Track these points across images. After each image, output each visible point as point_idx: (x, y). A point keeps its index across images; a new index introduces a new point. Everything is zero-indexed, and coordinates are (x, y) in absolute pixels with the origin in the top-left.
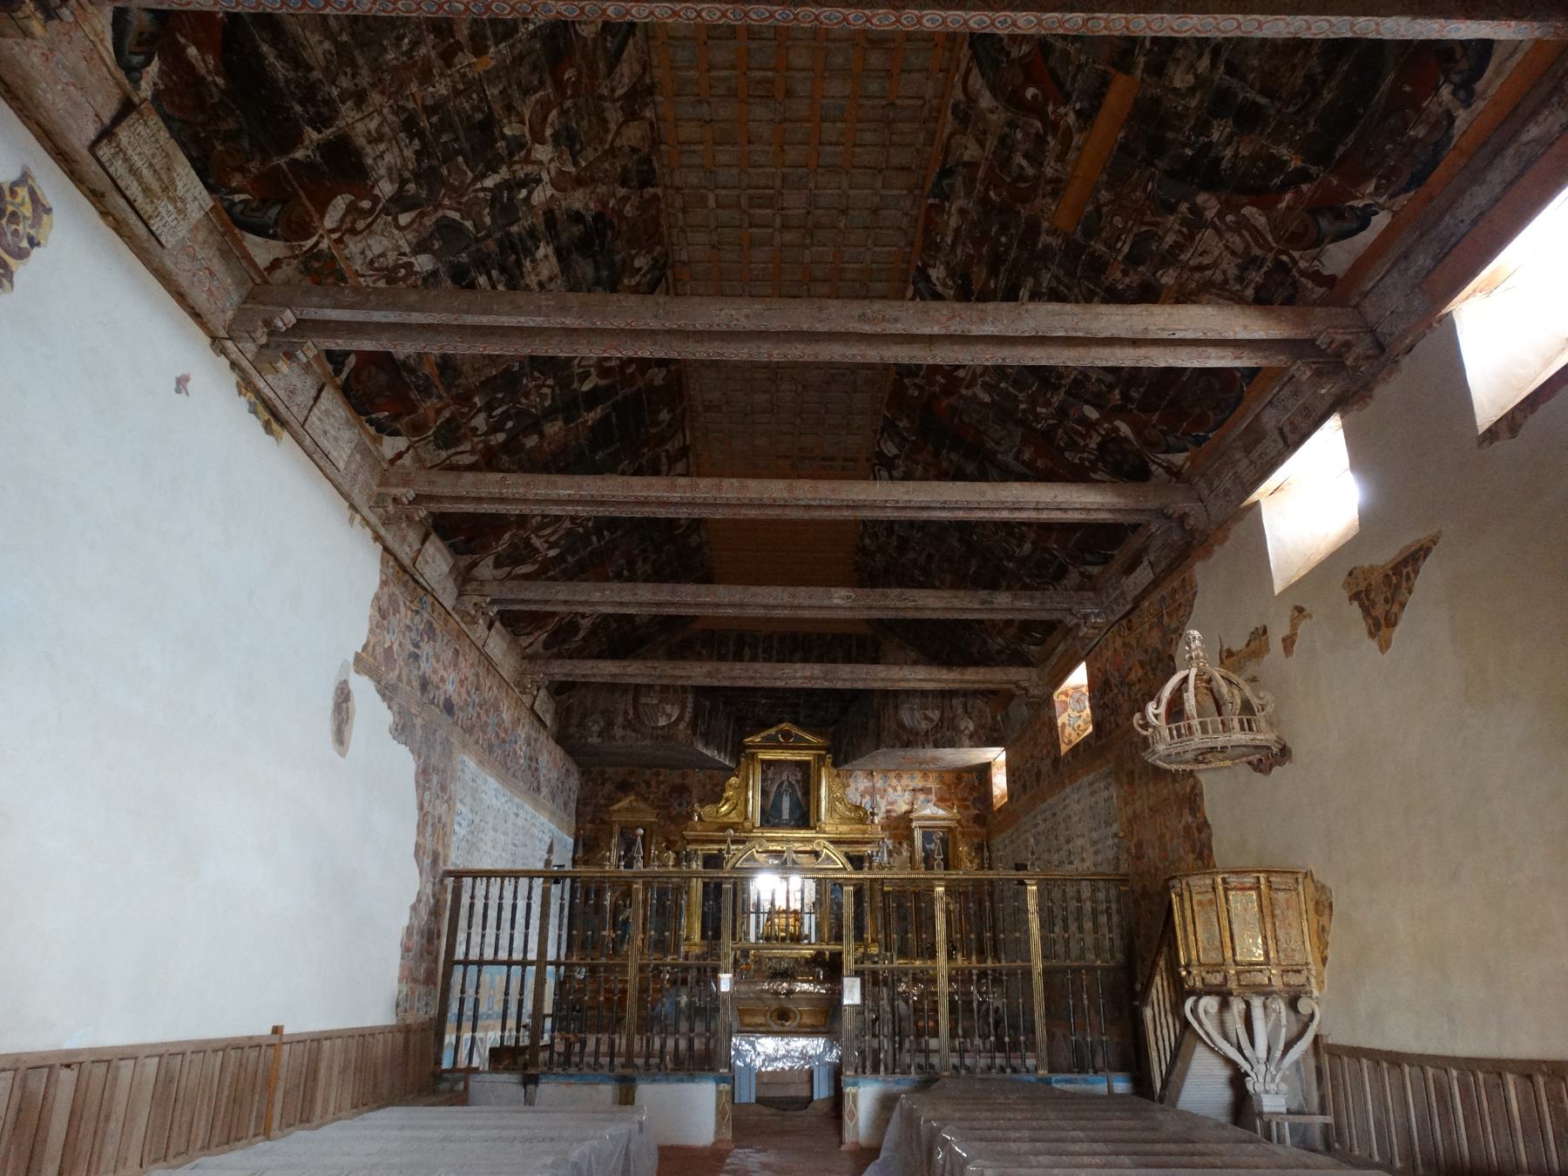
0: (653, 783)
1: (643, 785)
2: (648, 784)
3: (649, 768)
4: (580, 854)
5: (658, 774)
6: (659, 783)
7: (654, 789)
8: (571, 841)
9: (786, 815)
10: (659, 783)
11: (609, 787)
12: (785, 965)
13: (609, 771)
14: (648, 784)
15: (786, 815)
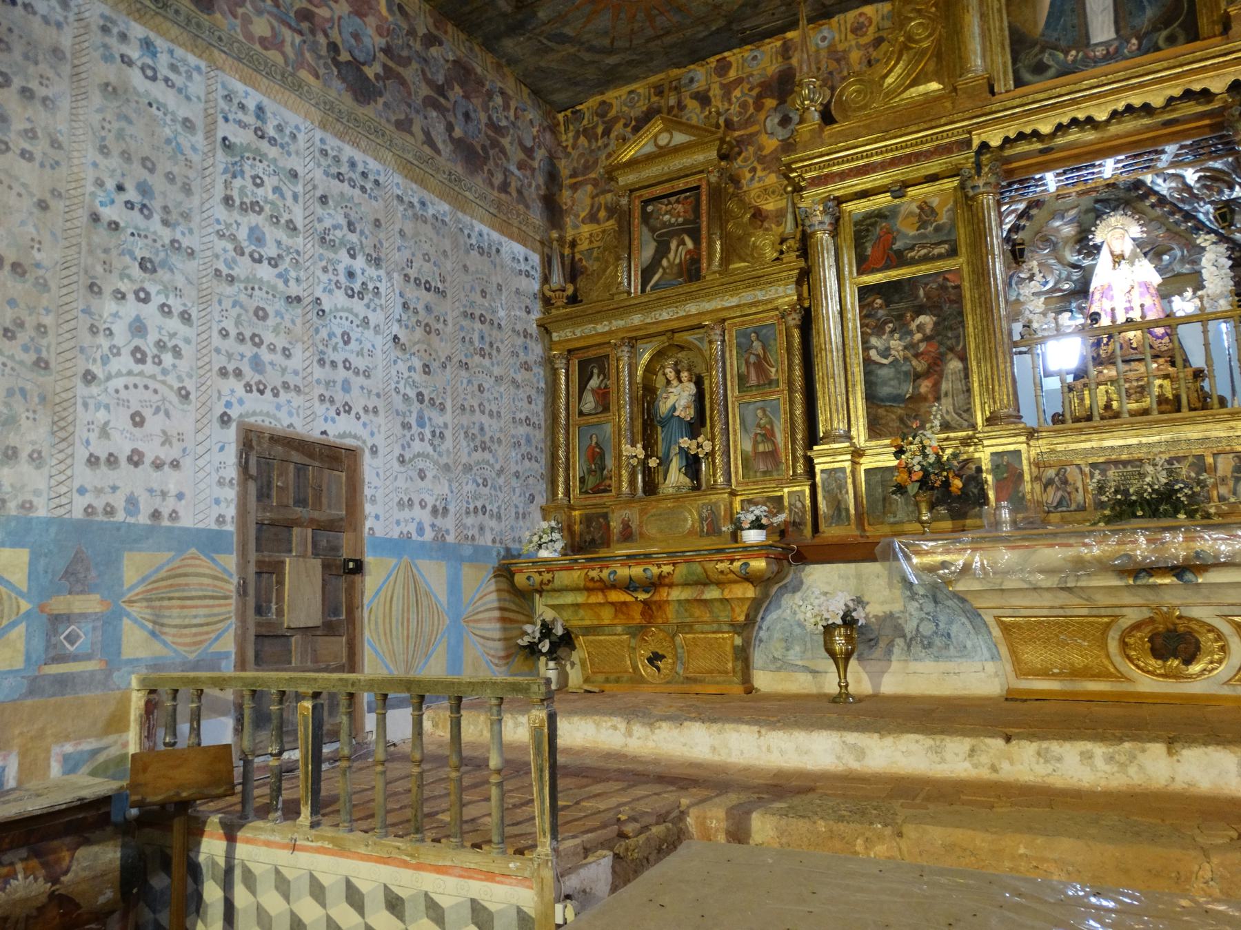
0: (715, 91)
1: (692, 105)
2: (703, 99)
3: (696, 55)
4: (557, 279)
5: (723, 68)
6: (727, 89)
7: (717, 103)
8: (535, 258)
9: (1102, 29)
10: (727, 89)
11: (618, 129)
12: (1155, 477)
13: (616, 96)
14: (703, 99)
15: (1102, 29)
